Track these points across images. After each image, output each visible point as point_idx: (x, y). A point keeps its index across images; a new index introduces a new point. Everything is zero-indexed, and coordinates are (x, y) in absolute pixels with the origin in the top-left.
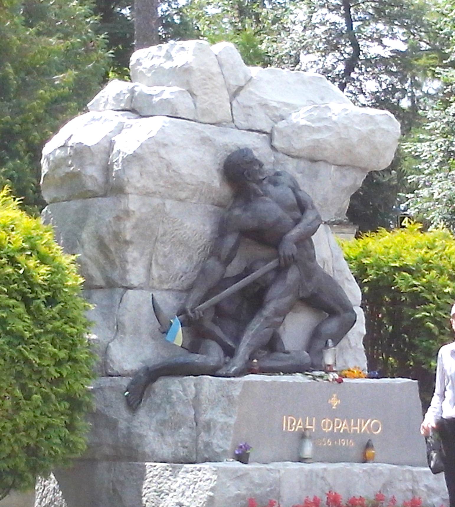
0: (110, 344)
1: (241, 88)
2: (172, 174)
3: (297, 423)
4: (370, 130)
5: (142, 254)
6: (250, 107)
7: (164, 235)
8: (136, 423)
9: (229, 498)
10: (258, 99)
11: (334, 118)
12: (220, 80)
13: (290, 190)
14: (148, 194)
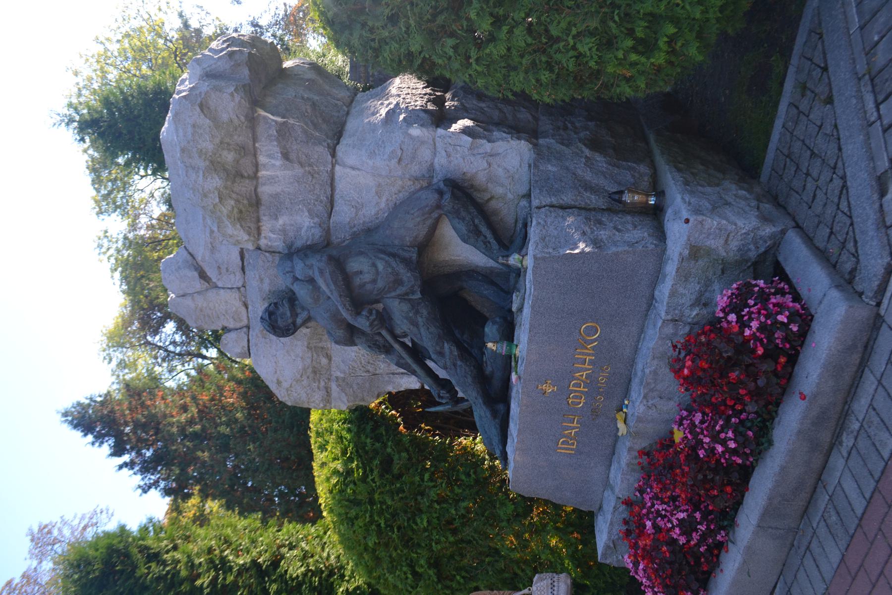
1: (203, 276)
2: (304, 377)
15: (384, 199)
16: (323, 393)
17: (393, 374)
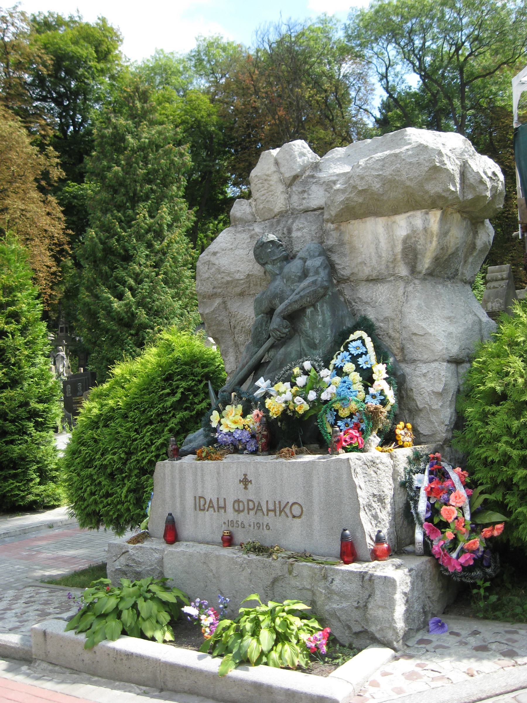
4: (393, 170)
15: (382, 324)
16: (211, 291)
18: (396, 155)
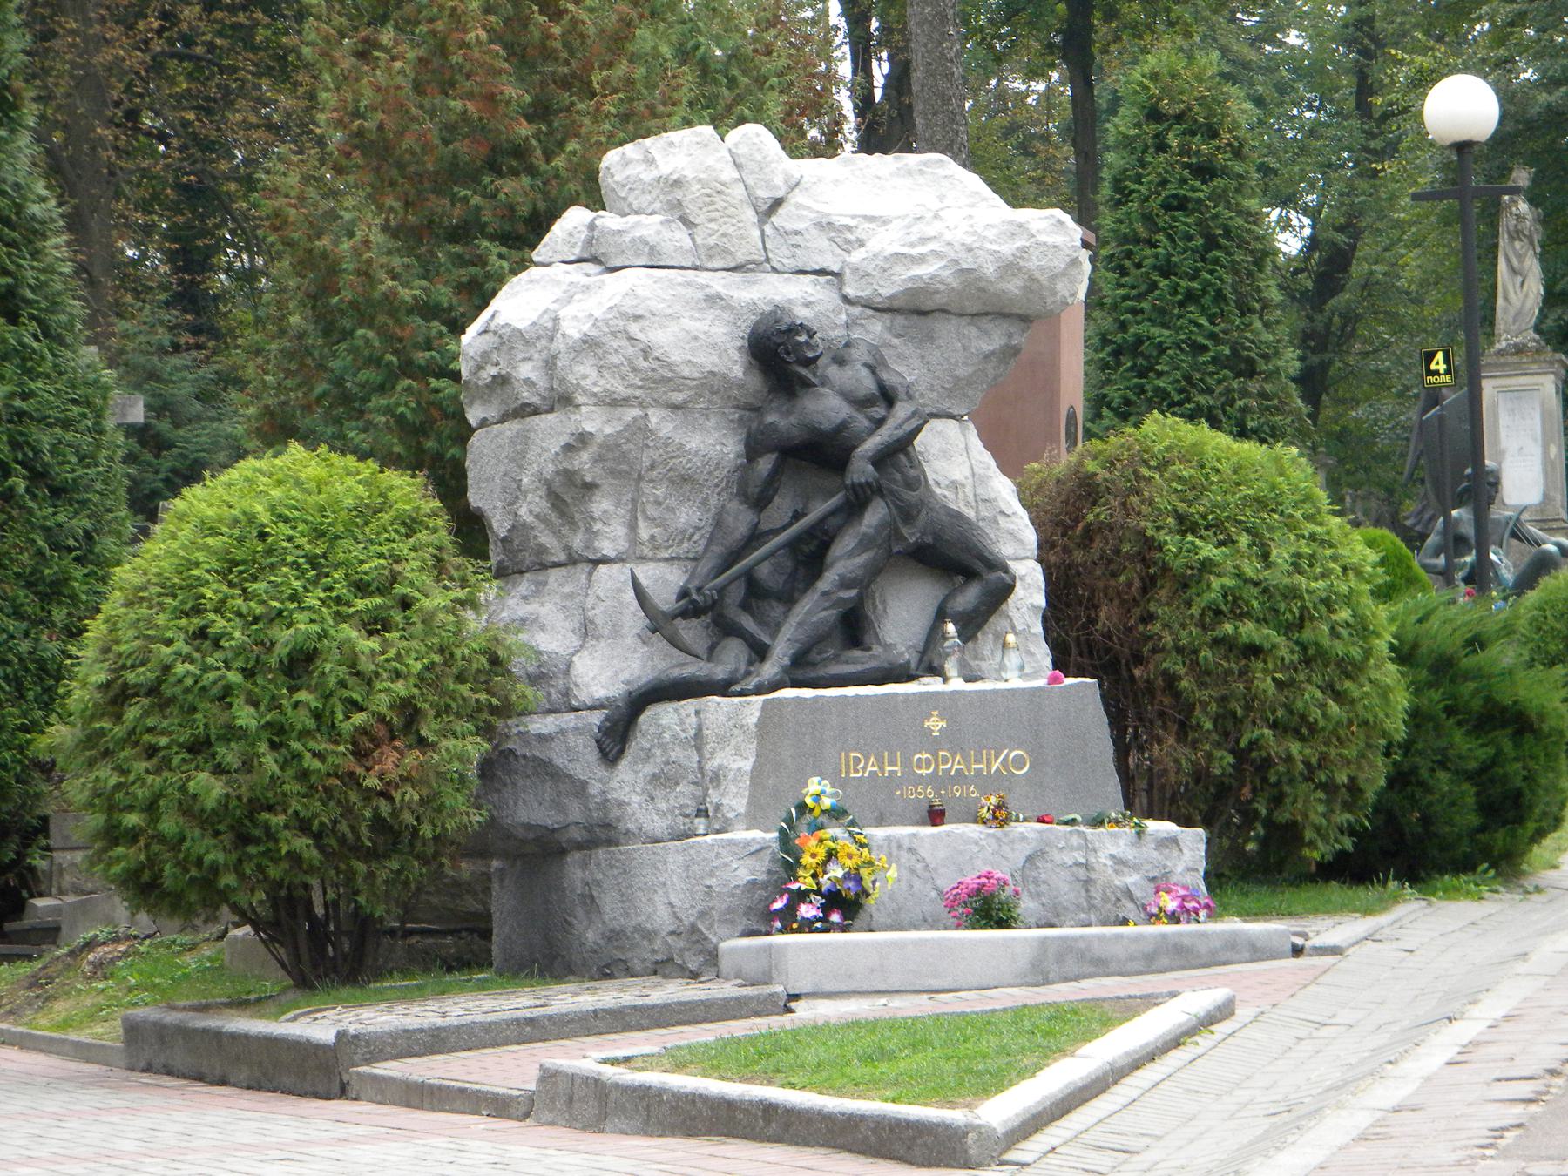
0: (575, 659)
1: (778, 203)
2: (655, 364)
3: (866, 764)
5: (618, 504)
6: (798, 233)
7: (652, 467)
8: (613, 784)
9: (737, 887)
10: (812, 216)
11: (948, 236)
12: (739, 191)
13: (865, 372)
14: (613, 402)
16: (621, 390)
17: (633, 512)
18: (1021, 226)
